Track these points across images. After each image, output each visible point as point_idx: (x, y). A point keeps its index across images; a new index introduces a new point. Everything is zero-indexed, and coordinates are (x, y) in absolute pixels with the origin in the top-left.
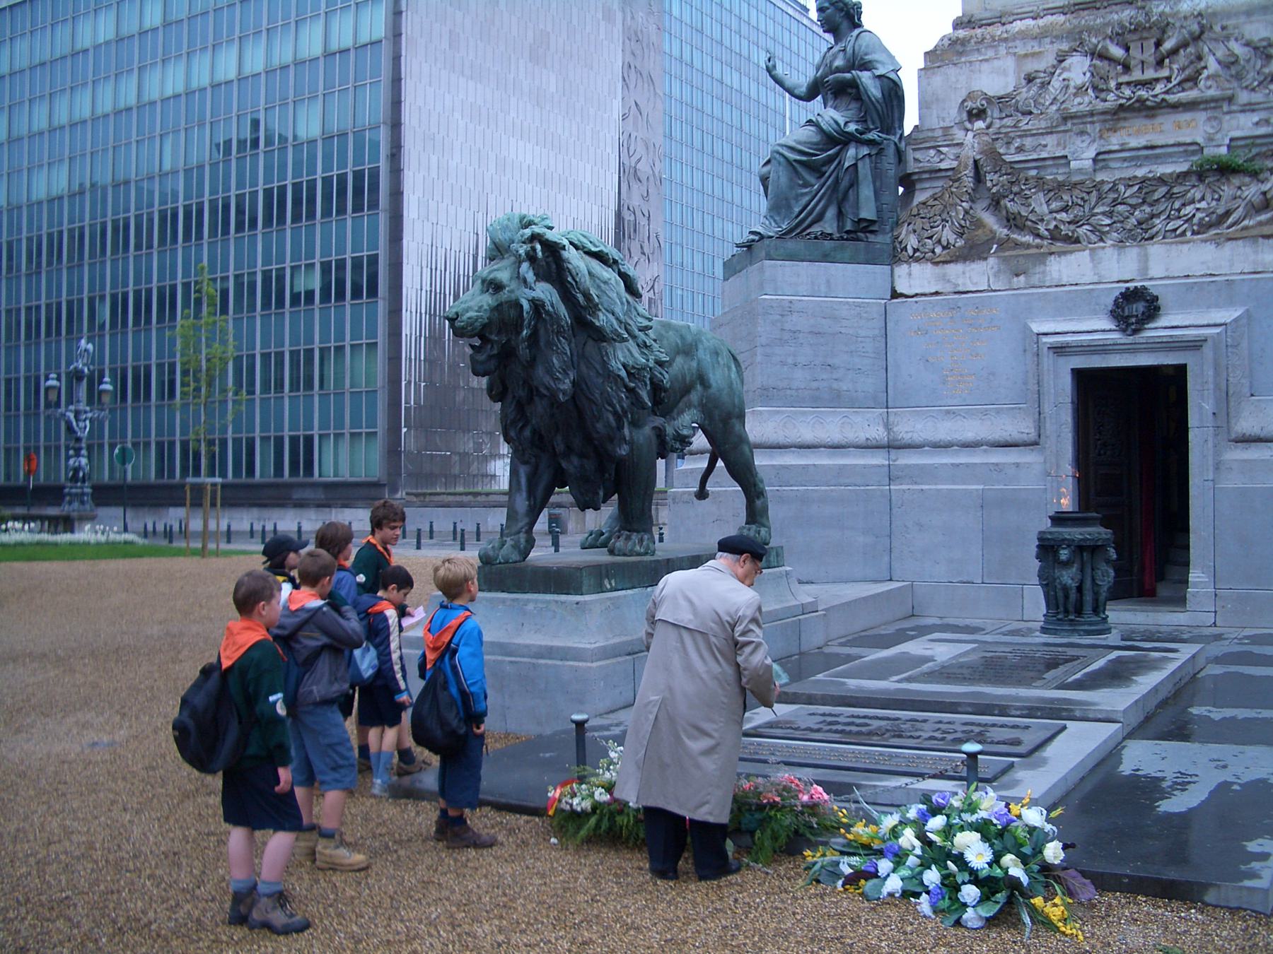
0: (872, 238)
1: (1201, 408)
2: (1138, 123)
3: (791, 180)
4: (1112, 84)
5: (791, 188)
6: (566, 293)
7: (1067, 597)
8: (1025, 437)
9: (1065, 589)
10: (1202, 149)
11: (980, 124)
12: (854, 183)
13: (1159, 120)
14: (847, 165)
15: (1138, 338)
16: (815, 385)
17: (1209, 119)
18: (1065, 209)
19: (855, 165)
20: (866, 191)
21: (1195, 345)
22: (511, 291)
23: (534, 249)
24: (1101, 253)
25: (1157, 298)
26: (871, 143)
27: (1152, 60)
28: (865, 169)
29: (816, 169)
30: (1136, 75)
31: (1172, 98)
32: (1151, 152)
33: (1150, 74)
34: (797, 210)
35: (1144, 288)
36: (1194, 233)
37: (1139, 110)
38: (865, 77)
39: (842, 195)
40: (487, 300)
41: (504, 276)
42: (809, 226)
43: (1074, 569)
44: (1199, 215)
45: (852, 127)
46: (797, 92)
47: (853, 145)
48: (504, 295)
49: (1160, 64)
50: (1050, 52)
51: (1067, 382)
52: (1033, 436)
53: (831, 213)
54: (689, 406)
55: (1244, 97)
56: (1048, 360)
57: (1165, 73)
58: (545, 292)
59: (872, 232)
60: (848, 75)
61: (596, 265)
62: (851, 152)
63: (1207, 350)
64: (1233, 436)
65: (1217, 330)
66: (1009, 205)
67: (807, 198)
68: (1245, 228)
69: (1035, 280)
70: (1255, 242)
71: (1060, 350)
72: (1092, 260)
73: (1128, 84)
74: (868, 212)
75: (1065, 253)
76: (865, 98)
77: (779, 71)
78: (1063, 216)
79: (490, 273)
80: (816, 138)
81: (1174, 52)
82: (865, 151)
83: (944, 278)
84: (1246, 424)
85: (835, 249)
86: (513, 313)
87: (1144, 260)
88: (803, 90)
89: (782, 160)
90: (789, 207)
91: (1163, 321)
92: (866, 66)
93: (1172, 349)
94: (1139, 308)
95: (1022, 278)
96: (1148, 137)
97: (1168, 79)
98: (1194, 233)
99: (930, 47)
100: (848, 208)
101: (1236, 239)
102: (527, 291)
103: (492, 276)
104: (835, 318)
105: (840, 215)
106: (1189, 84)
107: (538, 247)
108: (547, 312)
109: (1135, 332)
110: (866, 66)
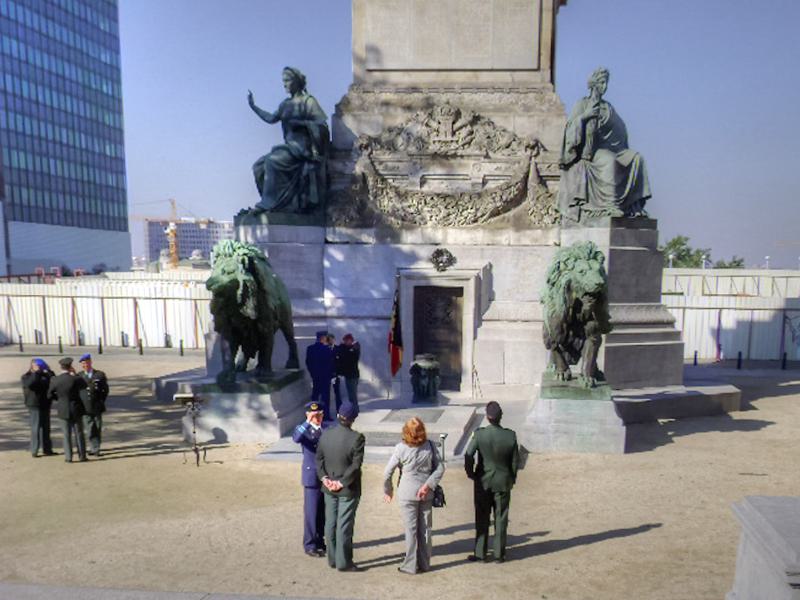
9: (424, 387)
15: (443, 273)
19: (308, 175)
20: (313, 188)
26: (316, 162)
28: (313, 176)
30: (442, 138)
31: (460, 152)
33: (449, 138)
34: (279, 195)
38: (311, 124)
39: (301, 187)
43: (427, 379)
45: (307, 153)
49: (454, 133)
51: (411, 291)
53: (295, 199)
57: (455, 139)
60: (302, 123)
74: (314, 199)
77: (256, 104)
82: (312, 166)
88: (271, 119)
91: (456, 266)
92: (312, 118)
97: (457, 142)
99: (338, 102)
105: (300, 200)
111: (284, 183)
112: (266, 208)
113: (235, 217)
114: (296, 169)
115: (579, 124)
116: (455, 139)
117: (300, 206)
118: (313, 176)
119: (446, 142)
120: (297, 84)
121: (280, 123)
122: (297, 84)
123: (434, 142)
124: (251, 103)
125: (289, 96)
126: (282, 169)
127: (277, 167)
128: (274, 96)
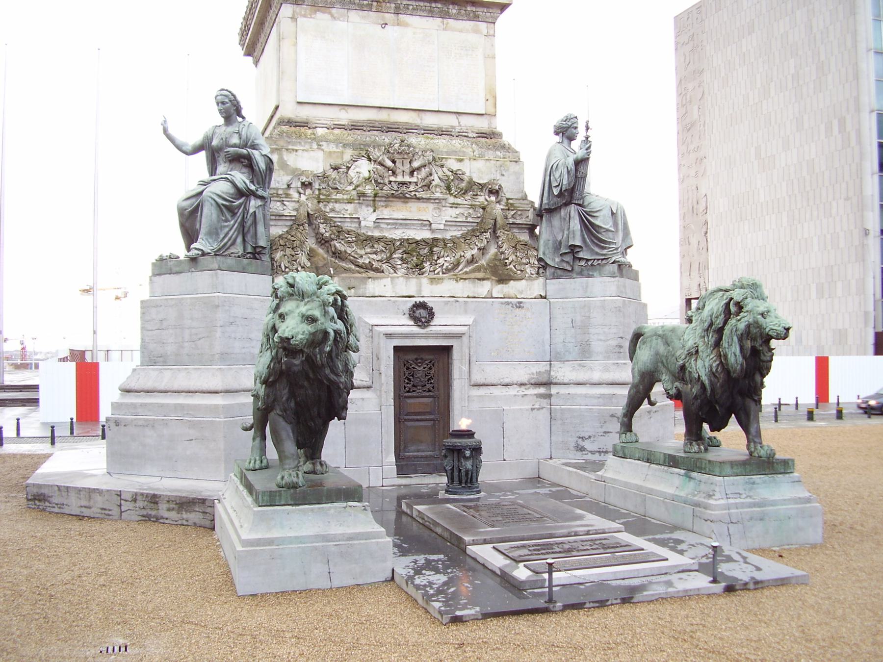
1: (460, 369)
2: (399, 204)
3: (218, 216)
4: (386, 181)
5: (218, 221)
7: (467, 474)
8: (365, 384)
10: (431, 224)
11: (308, 191)
12: (255, 222)
14: (251, 210)
16: (244, 351)
17: (435, 209)
18: (375, 253)
21: (459, 336)
22: (322, 324)
23: (336, 300)
24: (397, 280)
25: (432, 309)
27: (408, 171)
28: (259, 216)
29: (232, 211)
30: (400, 179)
32: (405, 223)
33: (407, 179)
34: (222, 236)
35: (424, 302)
36: (443, 273)
37: (400, 198)
40: (308, 328)
41: (317, 313)
42: (229, 248)
44: (446, 264)
46: (184, 148)
47: (252, 198)
48: (319, 326)
49: (412, 173)
50: (348, 154)
52: (369, 383)
53: (240, 240)
55: (452, 200)
56: (383, 340)
58: (340, 325)
60: (244, 151)
63: (465, 339)
64: (472, 383)
65: (466, 328)
66: (337, 245)
67: (227, 229)
68: (466, 273)
69: (361, 292)
70: (474, 282)
71: (389, 336)
72: (392, 283)
73: (395, 182)
75: (377, 278)
76: (256, 168)
77: (171, 131)
78: (374, 256)
79: (308, 310)
80: (232, 191)
81: (419, 169)
84: (477, 378)
85: (248, 264)
86: (321, 336)
88: (189, 148)
89: (213, 202)
90: (217, 234)
91: (435, 321)
94: (422, 312)
95: (353, 290)
96: (403, 213)
98: (443, 273)
100: (249, 238)
101: (465, 279)
102: (332, 324)
103: (310, 313)
104: (252, 309)
105: (244, 241)
106: (426, 188)
107: (339, 298)
108: (341, 337)
109: (425, 327)
110: (254, 147)
111: (227, 221)
112: (207, 250)
113: (153, 264)
114: (241, 205)
115: (571, 166)
116: (414, 180)
117: (244, 250)
119: (403, 183)
120: (231, 110)
121: (203, 155)
122: (231, 110)
123: (390, 182)
124: (165, 131)
125: (221, 121)
126: (224, 203)
127: (221, 201)
128: (207, 121)
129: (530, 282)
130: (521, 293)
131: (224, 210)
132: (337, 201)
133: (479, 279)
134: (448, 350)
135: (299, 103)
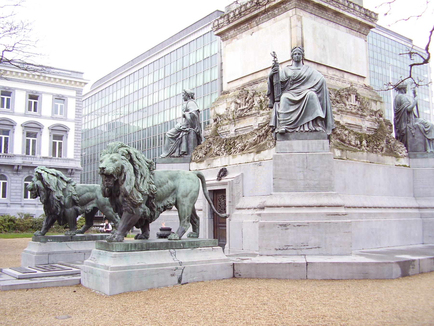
0: (185, 156)
2: (242, 120)
6: (43, 184)
12: (181, 143)
13: (246, 119)
17: (255, 119)
26: (186, 131)
28: (184, 138)
33: (244, 107)
44: (239, 147)
54: (93, 203)
59: (186, 155)
61: (51, 177)
62: (181, 134)
70: (247, 155)
82: (185, 133)
83: (197, 166)
85: (175, 160)
87: (229, 160)
93: (211, 186)
118: (184, 138)
126: (170, 136)
129: (269, 150)
130: (266, 157)
131: (171, 140)
132: (223, 125)
133: (249, 153)
134: (224, 191)
135: (228, 83)
